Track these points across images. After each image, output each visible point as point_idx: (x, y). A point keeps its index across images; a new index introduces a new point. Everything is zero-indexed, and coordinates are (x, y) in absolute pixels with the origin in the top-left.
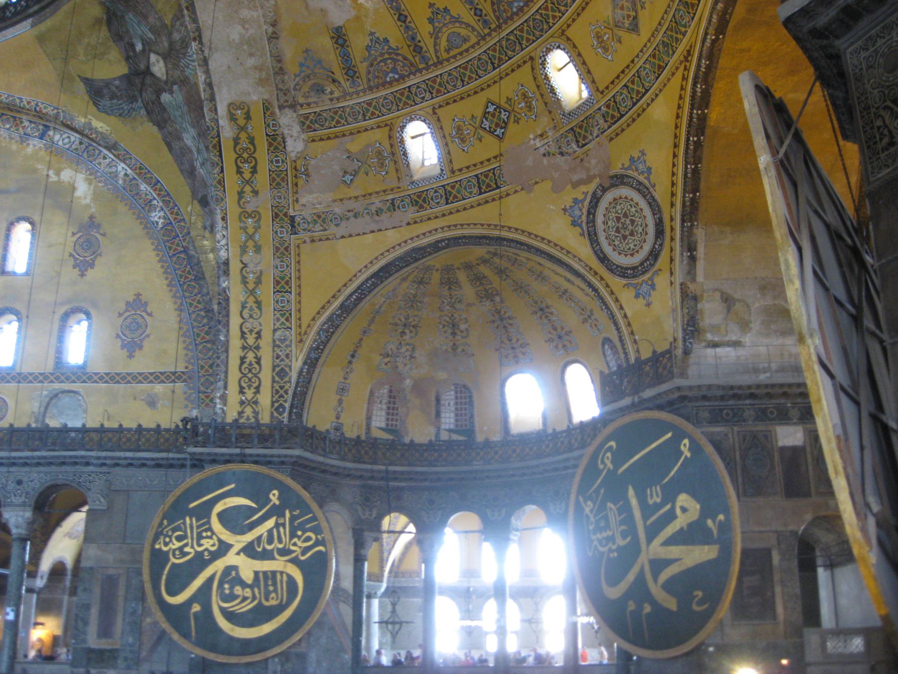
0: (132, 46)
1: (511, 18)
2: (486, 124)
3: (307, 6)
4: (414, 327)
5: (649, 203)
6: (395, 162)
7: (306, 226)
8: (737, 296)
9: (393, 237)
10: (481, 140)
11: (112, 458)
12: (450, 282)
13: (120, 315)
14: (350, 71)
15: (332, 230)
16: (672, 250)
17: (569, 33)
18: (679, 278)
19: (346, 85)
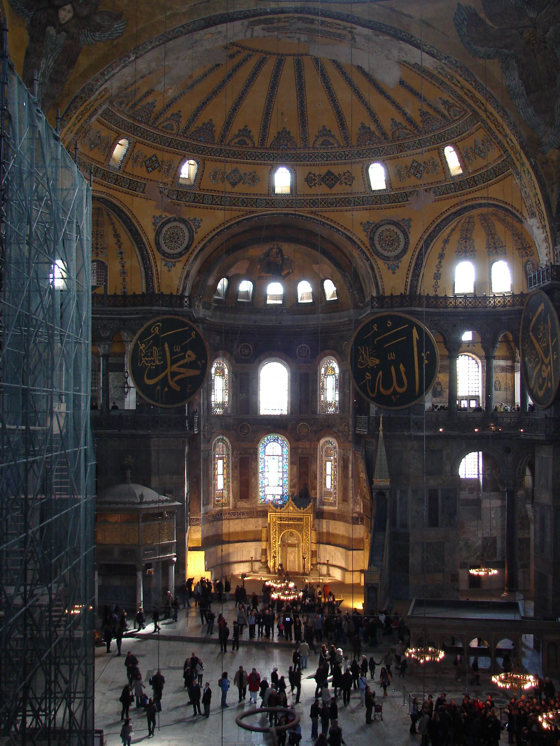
1: (194, 140)
2: (148, 163)
5: (190, 237)
10: (141, 166)
14: (135, 105)
16: (189, 257)
17: (206, 162)
18: (187, 268)
19: (127, 108)
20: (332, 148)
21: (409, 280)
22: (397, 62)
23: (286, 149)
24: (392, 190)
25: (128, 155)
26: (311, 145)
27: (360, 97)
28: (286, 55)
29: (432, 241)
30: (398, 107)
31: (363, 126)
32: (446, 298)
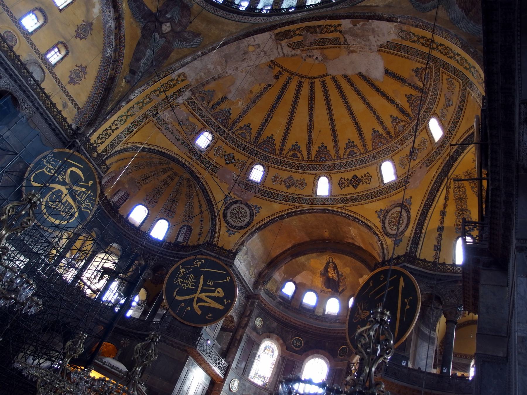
0: (167, 13)
1: (261, 149)
2: (226, 157)
3: (230, 86)
4: (140, 168)
5: (251, 218)
6: (195, 135)
7: (158, 119)
8: (248, 253)
9: (175, 149)
11: (44, 111)
12: (164, 171)
13: (76, 66)
14: (214, 107)
15: (163, 128)
16: (247, 231)
18: (243, 239)
19: (209, 107)
20: (356, 156)
21: (408, 249)
22: (379, 51)
23: (325, 161)
24: (398, 178)
25: (212, 145)
26: (342, 157)
27: (367, 103)
28: (314, 78)
29: (428, 211)
30: (392, 102)
31: (375, 132)
32: (444, 264)
